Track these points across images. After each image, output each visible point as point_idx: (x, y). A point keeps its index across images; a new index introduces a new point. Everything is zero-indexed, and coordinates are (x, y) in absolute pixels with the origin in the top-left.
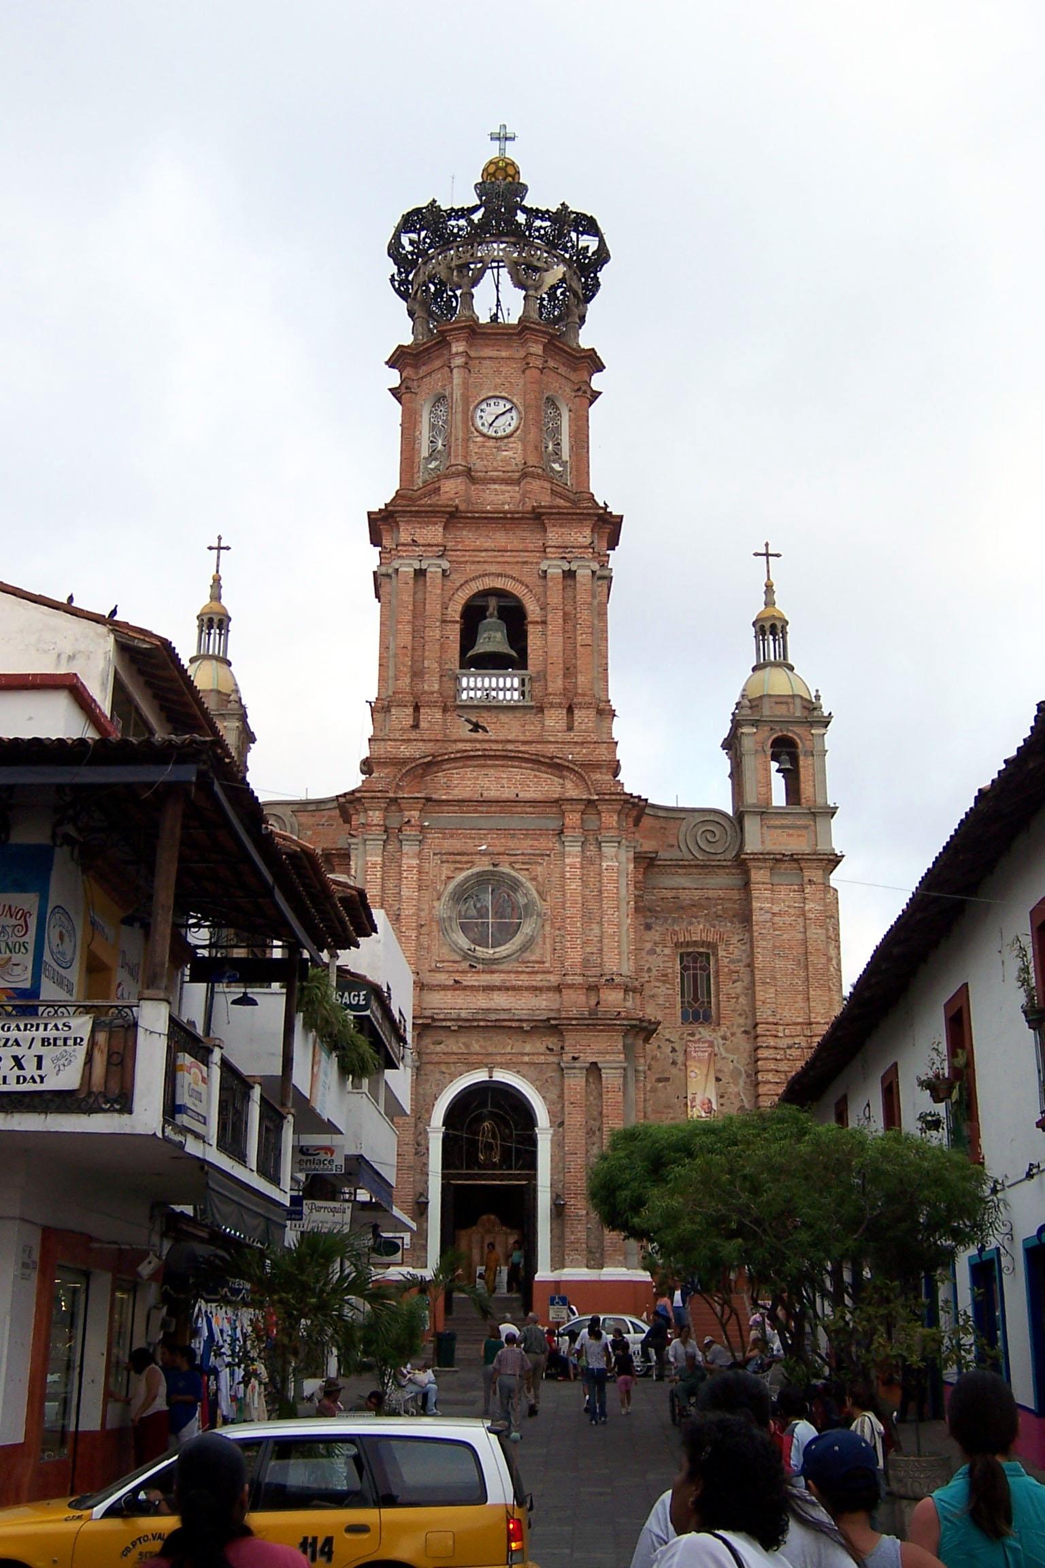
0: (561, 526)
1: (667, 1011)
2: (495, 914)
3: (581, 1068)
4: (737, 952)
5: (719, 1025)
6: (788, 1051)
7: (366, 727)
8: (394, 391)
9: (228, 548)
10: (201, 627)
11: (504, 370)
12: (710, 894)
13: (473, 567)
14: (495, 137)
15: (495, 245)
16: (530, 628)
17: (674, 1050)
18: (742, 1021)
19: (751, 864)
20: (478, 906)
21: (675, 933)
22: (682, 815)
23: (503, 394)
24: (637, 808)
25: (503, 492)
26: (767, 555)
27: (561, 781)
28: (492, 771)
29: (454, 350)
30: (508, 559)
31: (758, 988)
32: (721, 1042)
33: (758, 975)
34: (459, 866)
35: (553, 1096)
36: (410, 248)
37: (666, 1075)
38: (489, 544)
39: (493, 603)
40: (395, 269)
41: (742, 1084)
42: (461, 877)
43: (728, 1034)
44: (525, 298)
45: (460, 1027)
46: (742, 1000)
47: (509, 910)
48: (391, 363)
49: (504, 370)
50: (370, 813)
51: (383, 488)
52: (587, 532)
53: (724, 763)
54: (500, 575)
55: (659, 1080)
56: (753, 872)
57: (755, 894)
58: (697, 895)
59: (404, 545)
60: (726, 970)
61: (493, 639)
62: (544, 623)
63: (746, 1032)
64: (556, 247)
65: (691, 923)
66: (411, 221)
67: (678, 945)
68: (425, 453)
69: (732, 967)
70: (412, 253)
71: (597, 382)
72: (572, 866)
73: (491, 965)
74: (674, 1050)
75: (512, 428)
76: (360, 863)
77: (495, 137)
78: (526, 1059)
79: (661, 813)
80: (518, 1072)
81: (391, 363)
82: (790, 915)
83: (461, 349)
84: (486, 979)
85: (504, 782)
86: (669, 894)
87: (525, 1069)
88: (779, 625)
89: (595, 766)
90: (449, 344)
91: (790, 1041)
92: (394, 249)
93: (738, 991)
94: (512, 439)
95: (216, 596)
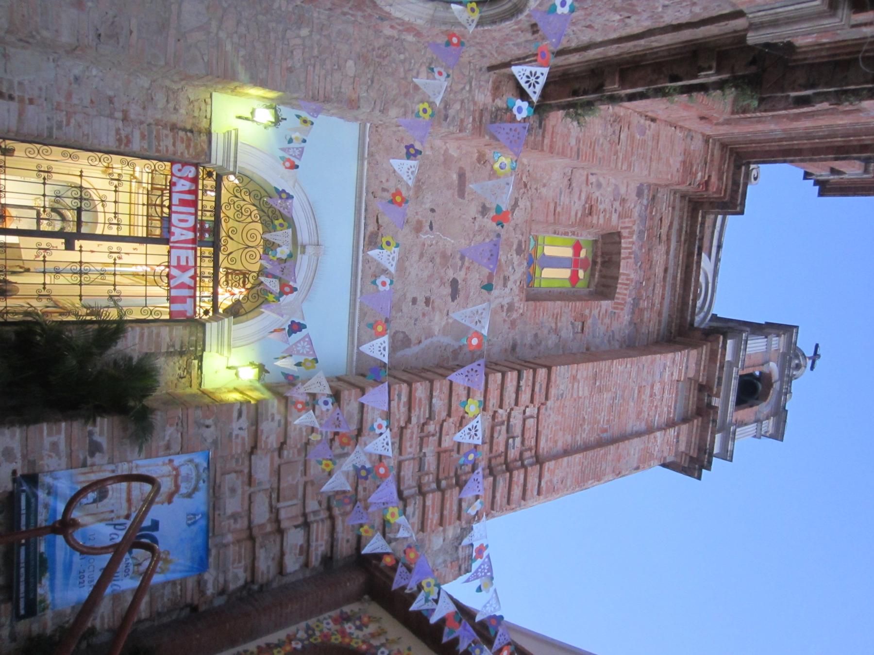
1: (552, 206)
4: (603, 329)
5: (527, 300)
6: (504, 428)
18: (529, 339)
19: (705, 349)
21: (631, 233)
31: (590, 365)
32: (506, 302)
33: (604, 365)
41: (446, 340)
43: (515, 315)
46: (552, 340)
55: (462, 176)
56: (694, 353)
57: (678, 355)
60: (587, 312)
63: (514, 347)
69: (589, 322)
82: (650, 408)
91: (518, 431)
93: (564, 333)
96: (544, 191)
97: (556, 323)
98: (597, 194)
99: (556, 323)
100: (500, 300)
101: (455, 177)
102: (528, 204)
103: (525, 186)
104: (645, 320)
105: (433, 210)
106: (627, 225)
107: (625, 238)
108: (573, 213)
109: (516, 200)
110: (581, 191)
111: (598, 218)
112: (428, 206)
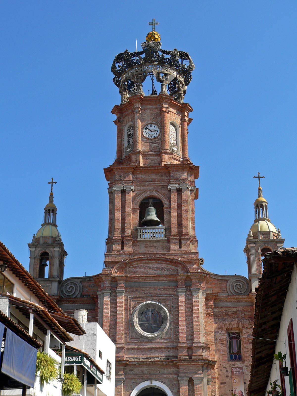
0: (176, 171)
1: (224, 355)
2: (153, 319)
3: (186, 380)
7: (103, 248)
8: (115, 122)
9: (56, 183)
10: (45, 212)
11: (154, 113)
12: (239, 309)
13: (143, 188)
14: (151, 24)
15: (150, 66)
16: (165, 210)
17: (227, 371)
20: (146, 316)
21: (226, 324)
22: (228, 279)
23: (154, 122)
24: (204, 276)
25: (154, 159)
26: (259, 177)
27: (177, 268)
28: (151, 265)
29: (135, 106)
30: (157, 184)
34: (139, 302)
35: (175, 390)
36: (118, 69)
37: (224, 382)
38: (149, 179)
39: (151, 201)
40: (114, 76)
42: (139, 306)
44: (161, 85)
45: (139, 364)
47: (158, 318)
48: (113, 112)
49: (154, 113)
50: (105, 282)
51: (110, 159)
52: (186, 174)
53: (244, 257)
54: (153, 191)
58: (234, 309)
59: (117, 181)
60: (246, 339)
61: (153, 216)
62: (170, 208)
64: (173, 65)
65: (232, 321)
66: (119, 58)
67: (227, 330)
68: (125, 144)
70: (120, 70)
71: (191, 115)
72: (182, 301)
73: (150, 340)
74: (227, 371)
75: (157, 135)
76: (101, 301)
77: (151, 24)
78: (165, 376)
79: (220, 278)
80: (162, 382)
81: (113, 112)
83: (137, 106)
84: (149, 346)
85: (155, 269)
86: (223, 309)
87: (163, 380)
88: (264, 204)
89: (191, 262)
90: (133, 105)
92: (113, 69)
94: (157, 139)
95: (51, 201)
96: (221, 359)
97: (250, 350)
98: (218, 339)
99: (250, 350)
100: (245, 369)
101: (222, 385)
102: (224, 363)
103: (220, 365)
104: (247, 313)
105: (229, 391)
106: (224, 327)
107: (227, 327)
108: (224, 348)
109: (224, 367)
110: (219, 346)
111: (224, 338)
112: (228, 392)
